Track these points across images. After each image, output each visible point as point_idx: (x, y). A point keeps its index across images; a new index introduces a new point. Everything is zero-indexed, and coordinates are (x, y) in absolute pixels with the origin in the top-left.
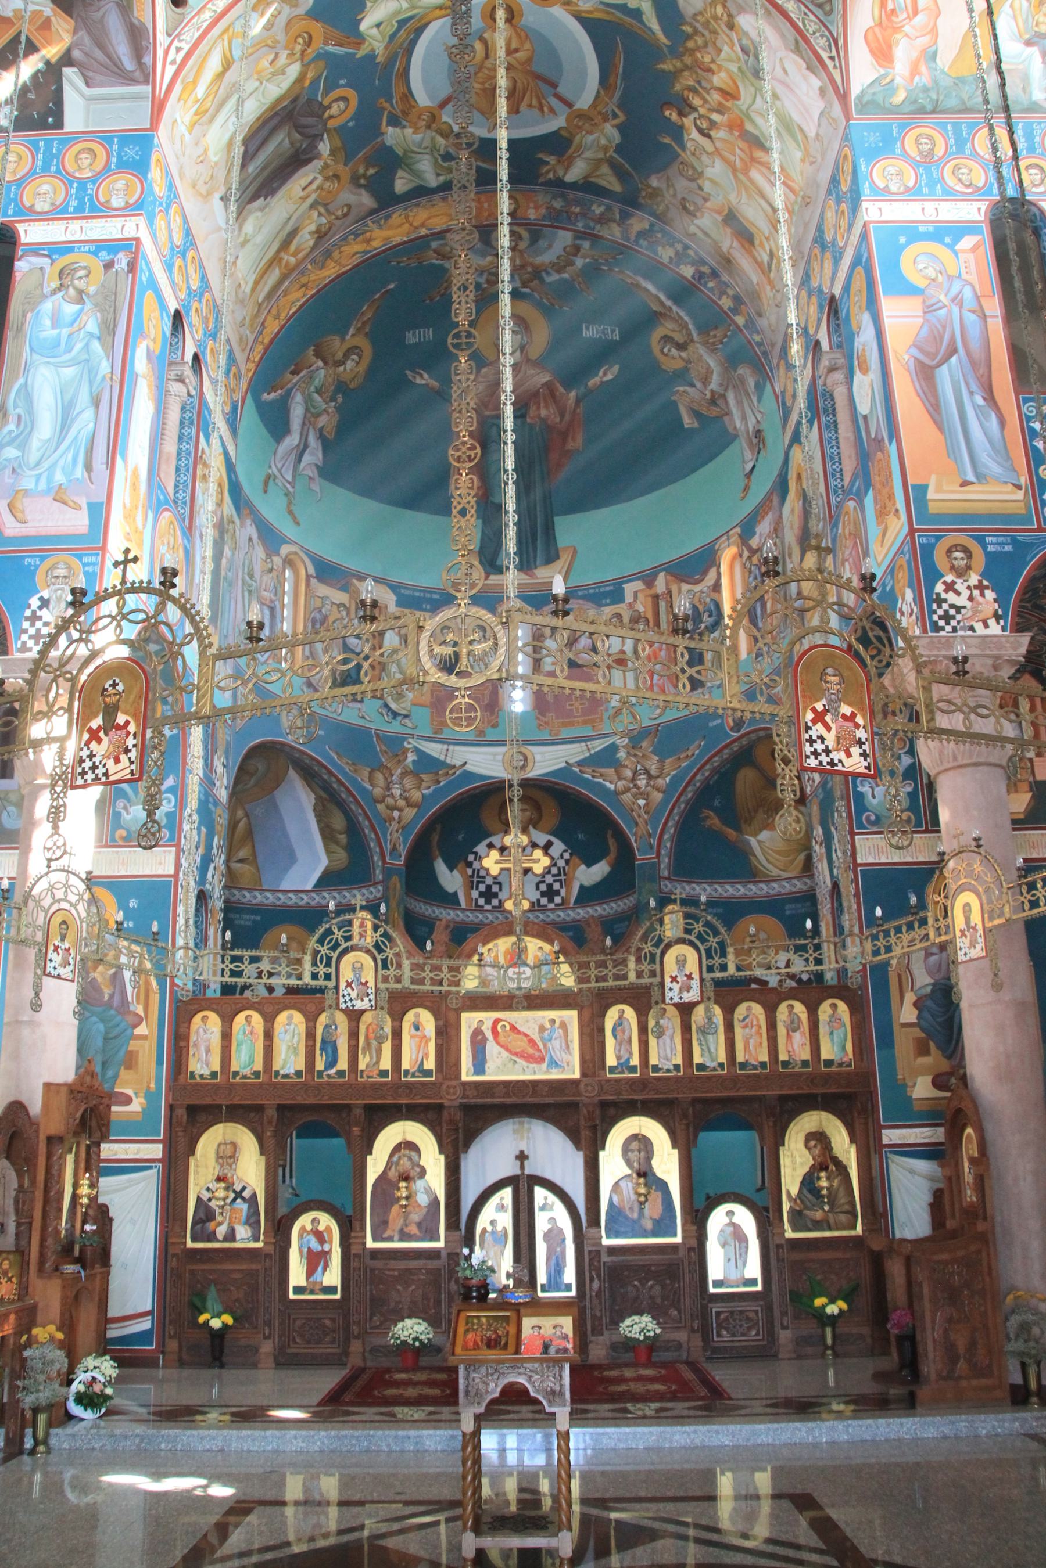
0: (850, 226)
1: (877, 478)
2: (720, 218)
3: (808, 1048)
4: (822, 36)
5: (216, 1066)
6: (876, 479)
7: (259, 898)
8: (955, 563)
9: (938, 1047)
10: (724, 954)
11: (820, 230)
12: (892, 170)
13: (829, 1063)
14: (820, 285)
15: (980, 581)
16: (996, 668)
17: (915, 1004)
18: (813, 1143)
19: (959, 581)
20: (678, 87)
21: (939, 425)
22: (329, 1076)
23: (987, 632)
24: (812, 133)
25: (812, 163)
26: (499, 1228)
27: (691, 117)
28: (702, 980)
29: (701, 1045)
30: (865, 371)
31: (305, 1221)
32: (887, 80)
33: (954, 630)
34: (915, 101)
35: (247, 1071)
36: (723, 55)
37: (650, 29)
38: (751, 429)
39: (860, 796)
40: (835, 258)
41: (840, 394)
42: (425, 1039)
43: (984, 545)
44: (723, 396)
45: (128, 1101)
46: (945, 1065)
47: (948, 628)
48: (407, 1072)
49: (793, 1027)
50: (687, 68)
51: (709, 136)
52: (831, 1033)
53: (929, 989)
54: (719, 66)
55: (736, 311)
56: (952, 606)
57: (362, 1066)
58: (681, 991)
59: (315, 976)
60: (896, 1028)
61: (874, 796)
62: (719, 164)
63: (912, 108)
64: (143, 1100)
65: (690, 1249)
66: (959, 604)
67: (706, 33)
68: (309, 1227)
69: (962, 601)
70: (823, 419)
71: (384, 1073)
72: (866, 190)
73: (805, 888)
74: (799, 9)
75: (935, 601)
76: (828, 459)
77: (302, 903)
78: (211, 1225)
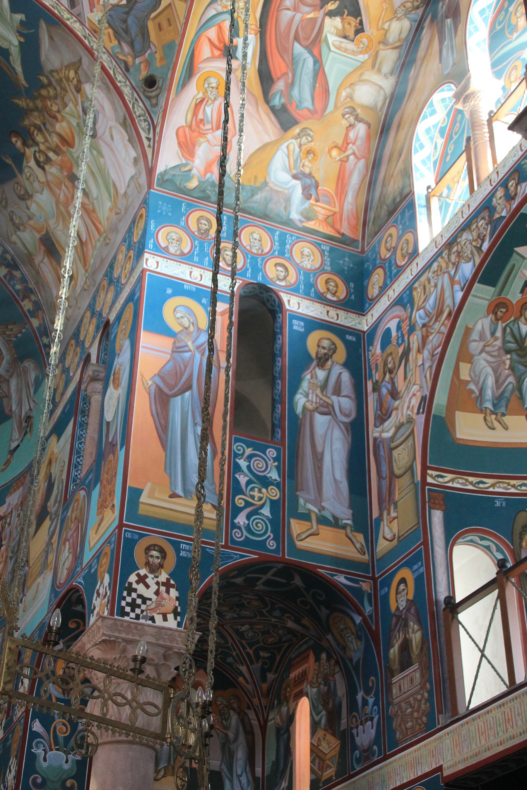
0: (133, 269)
1: (105, 476)
2: (38, 236)
4: (145, 120)
6: (104, 476)
8: (151, 560)
11: (111, 266)
12: (174, 236)
14: (101, 310)
15: (168, 580)
16: (166, 657)
19: (151, 576)
20: (27, 122)
21: (164, 445)
23: (166, 624)
24: (122, 191)
25: (117, 214)
27: (33, 149)
30: (117, 387)
32: (187, 169)
33: (138, 617)
34: (204, 191)
36: (67, 109)
37: (14, 69)
38: (23, 414)
39: (32, 757)
40: (116, 290)
41: (96, 399)
43: (178, 550)
44: (8, 381)
47: (133, 615)
50: (37, 109)
51: (43, 169)
54: (63, 117)
55: (33, 314)
56: (140, 596)
61: (45, 760)
62: (46, 192)
63: (200, 195)
66: (146, 595)
67: (58, 88)
69: (149, 593)
70: (79, 418)
72: (150, 244)
74: (132, 94)
75: (126, 589)
76: (75, 452)
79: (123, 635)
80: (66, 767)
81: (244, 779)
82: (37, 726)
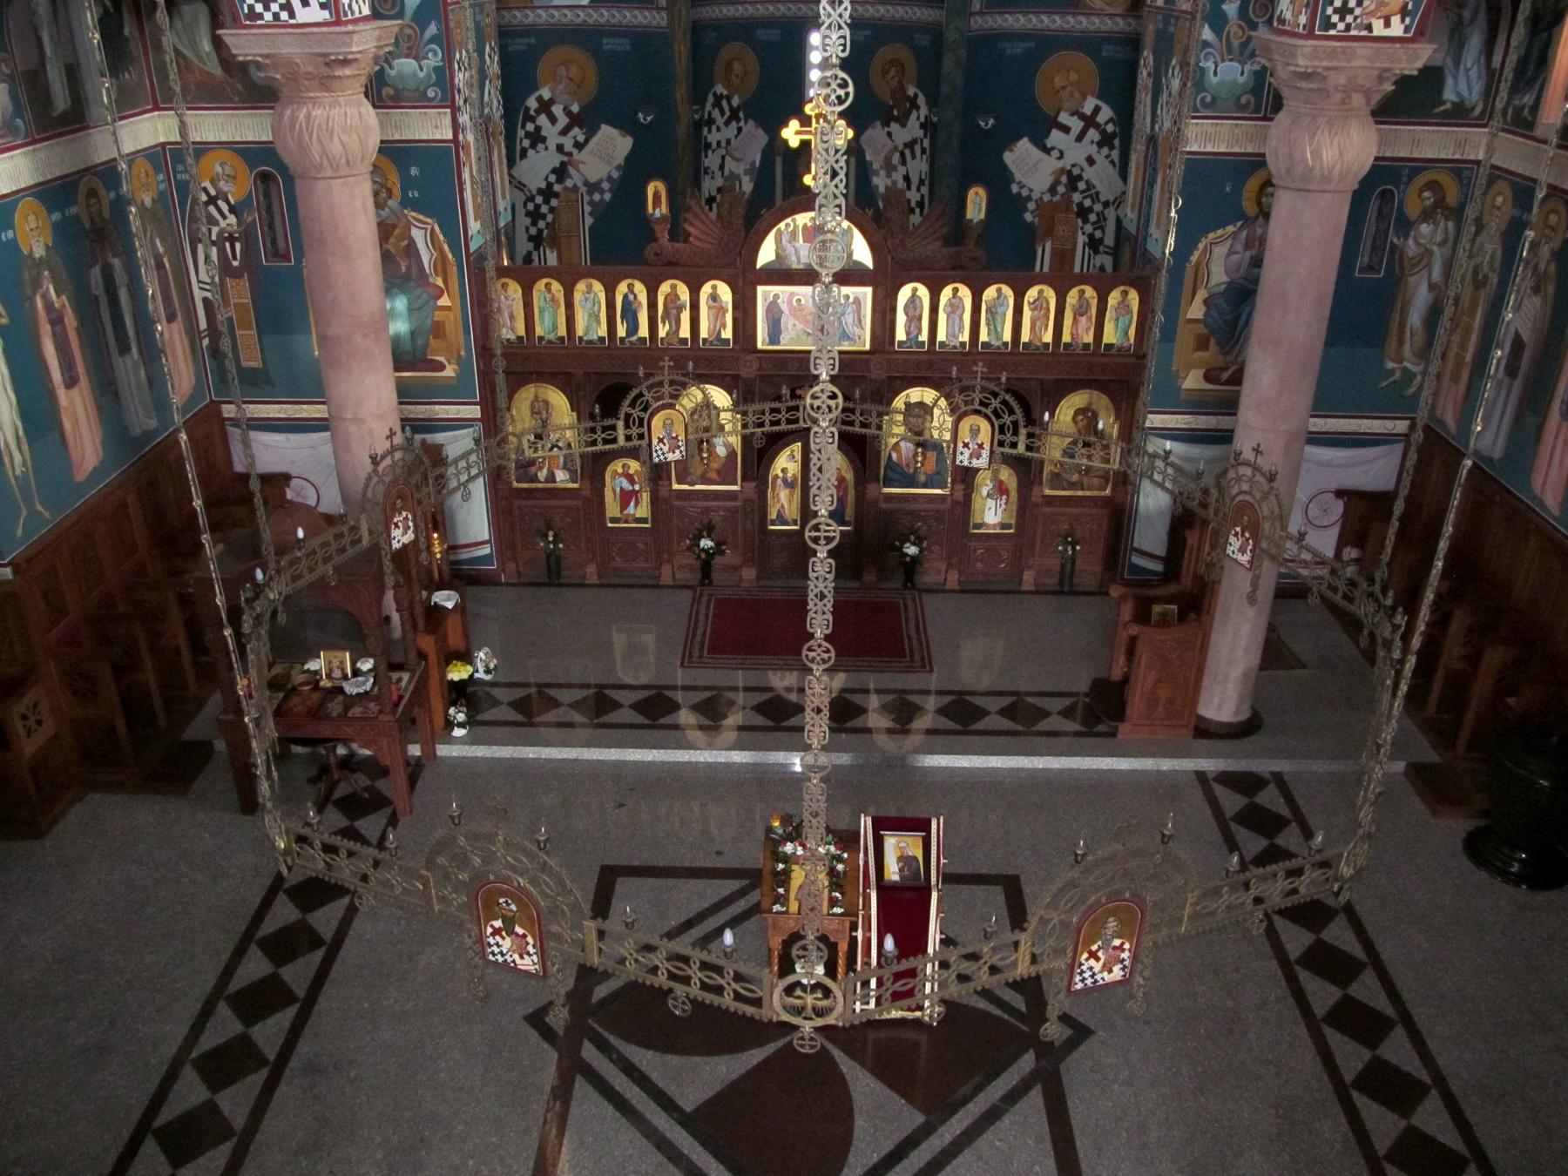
3: (1092, 333)
5: (522, 331)
7: (532, 17)
9: (1218, 344)
10: (1016, 433)
13: (1109, 346)
17: (1205, 302)
18: (1080, 417)
22: (631, 342)
26: (789, 475)
28: (992, 452)
29: (988, 324)
31: (617, 466)
33: (1348, 27)
35: (551, 337)
42: (721, 310)
45: (441, 367)
46: (1220, 361)
47: (1341, 26)
48: (705, 340)
49: (1081, 311)
52: (1117, 319)
53: (1224, 286)
57: (662, 333)
58: (971, 457)
59: (628, 438)
60: (1181, 320)
61: (1215, 73)
64: (455, 367)
65: (956, 503)
68: (620, 471)
71: (684, 341)
73: (1128, 29)
77: (578, 21)
78: (533, 469)
79: (1325, 63)
80: (1241, 80)
81: (1473, 74)
82: (1207, 34)
